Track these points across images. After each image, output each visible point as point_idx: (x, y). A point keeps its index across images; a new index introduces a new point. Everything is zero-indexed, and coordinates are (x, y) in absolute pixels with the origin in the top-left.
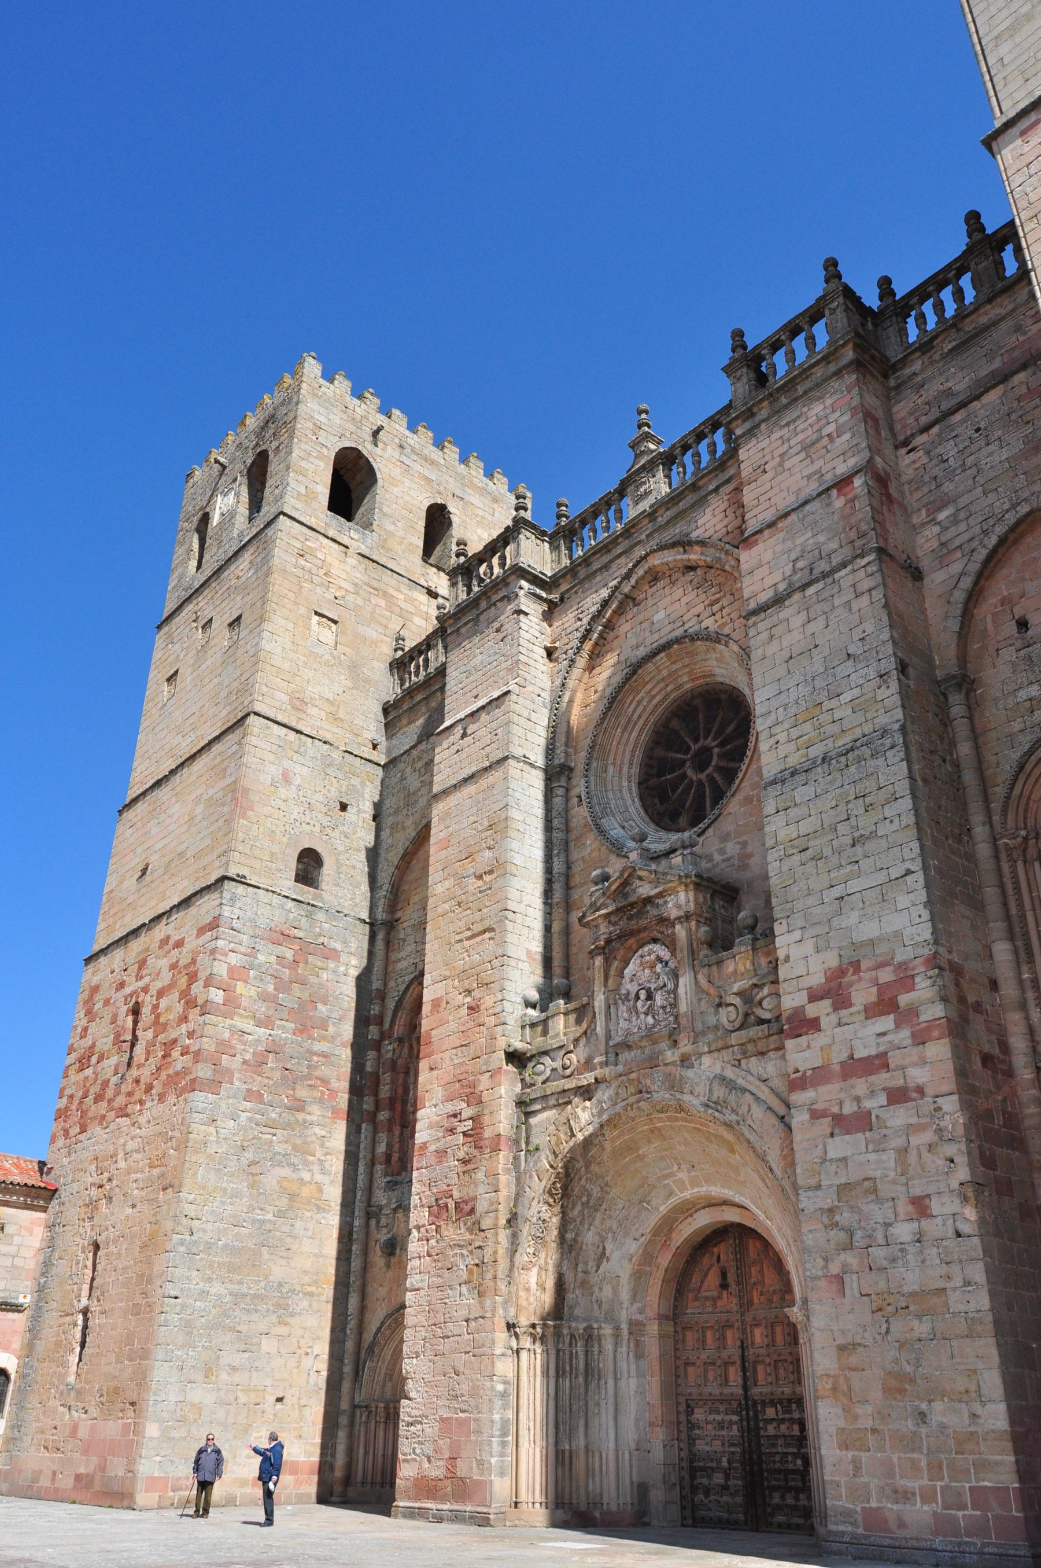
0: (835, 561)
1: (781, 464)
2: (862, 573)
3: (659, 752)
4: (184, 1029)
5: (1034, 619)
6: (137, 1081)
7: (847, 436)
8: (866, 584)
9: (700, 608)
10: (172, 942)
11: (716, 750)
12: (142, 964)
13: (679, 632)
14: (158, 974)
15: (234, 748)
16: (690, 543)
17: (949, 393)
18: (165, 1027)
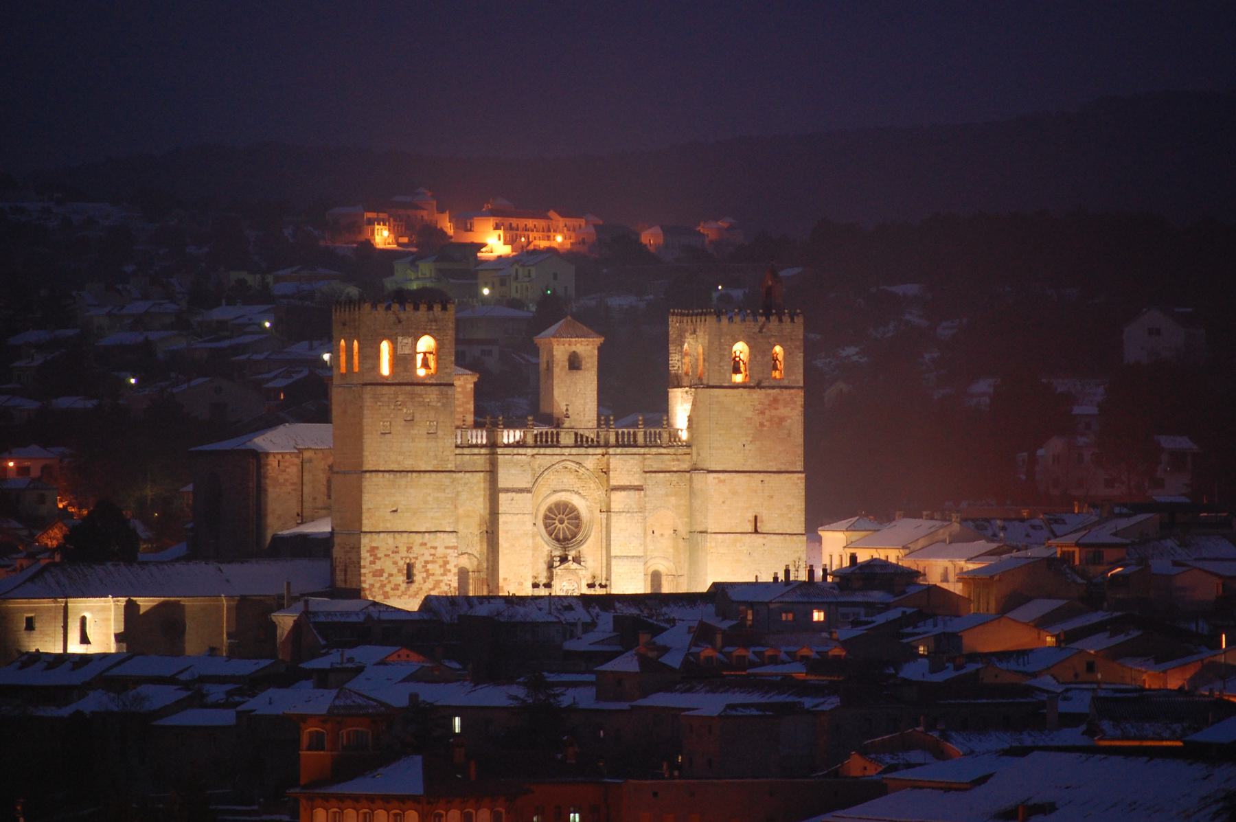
0: (635, 510)
1: (621, 472)
2: (640, 518)
3: (548, 513)
4: (445, 577)
5: (655, 532)
6: (421, 589)
7: (638, 475)
8: (641, 521)
9: (579, 486)
10: (429, 545)
11: (566, 522)
12: (409, 549)
13: (572, 489)
14: (423, 554)
15: (448, 484)
16: (583, 467)
17: (651, 466)
18: (433, 575)
